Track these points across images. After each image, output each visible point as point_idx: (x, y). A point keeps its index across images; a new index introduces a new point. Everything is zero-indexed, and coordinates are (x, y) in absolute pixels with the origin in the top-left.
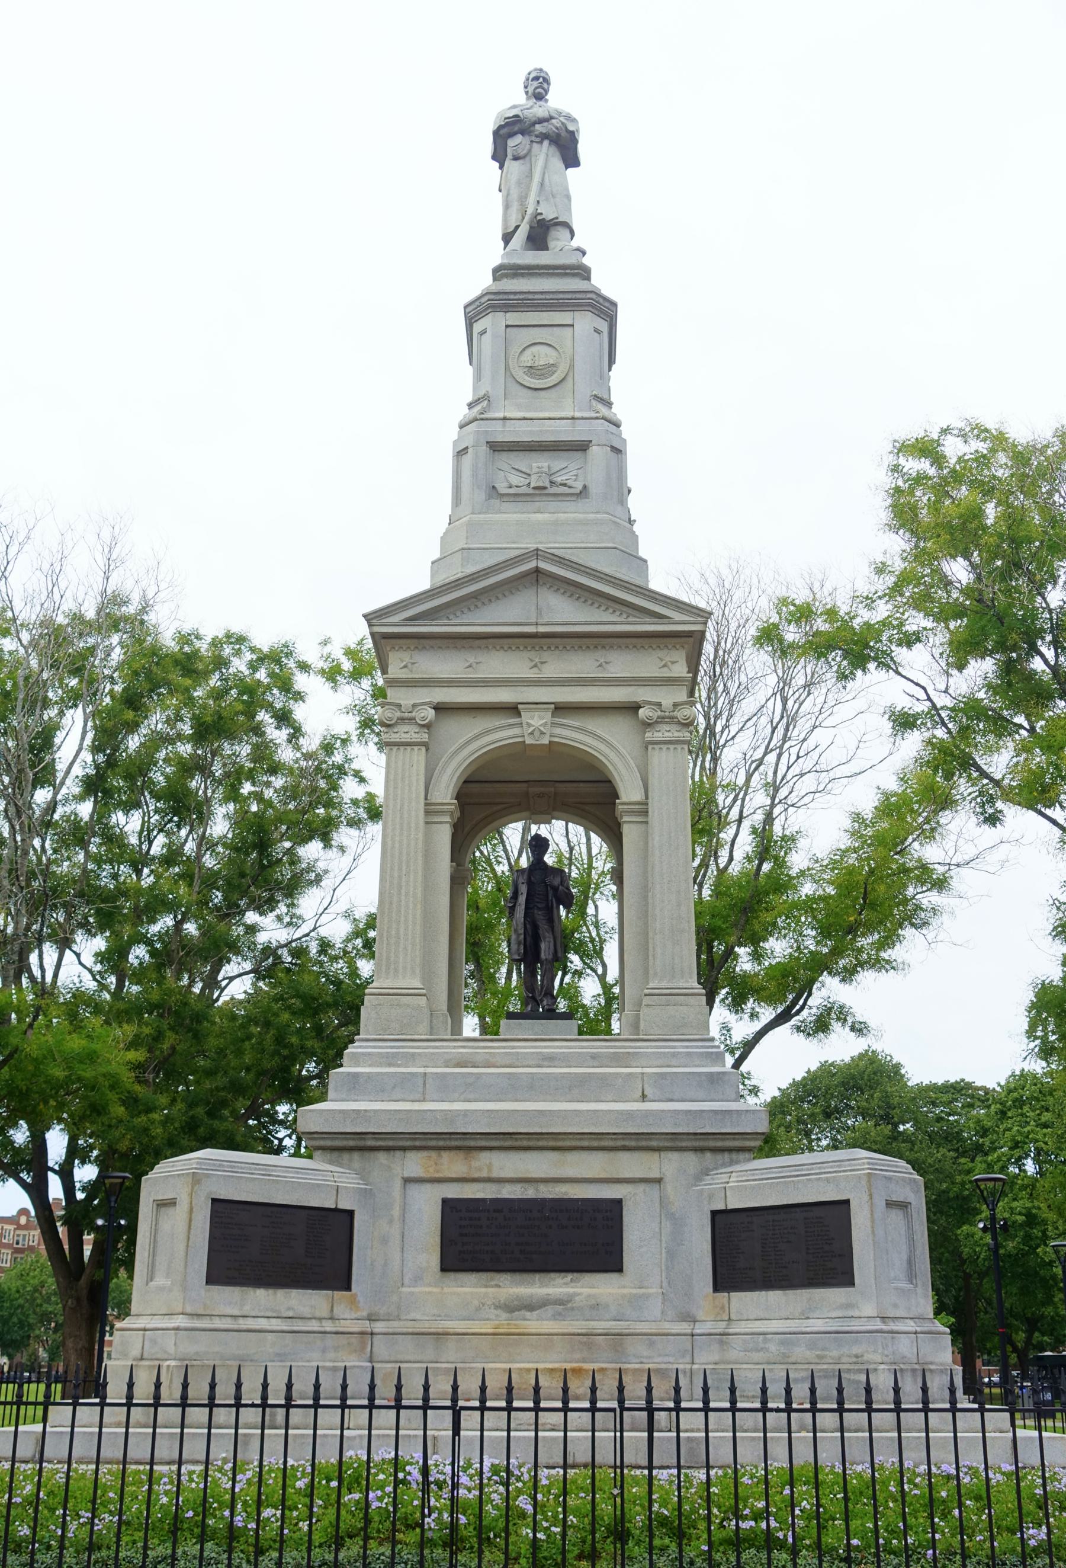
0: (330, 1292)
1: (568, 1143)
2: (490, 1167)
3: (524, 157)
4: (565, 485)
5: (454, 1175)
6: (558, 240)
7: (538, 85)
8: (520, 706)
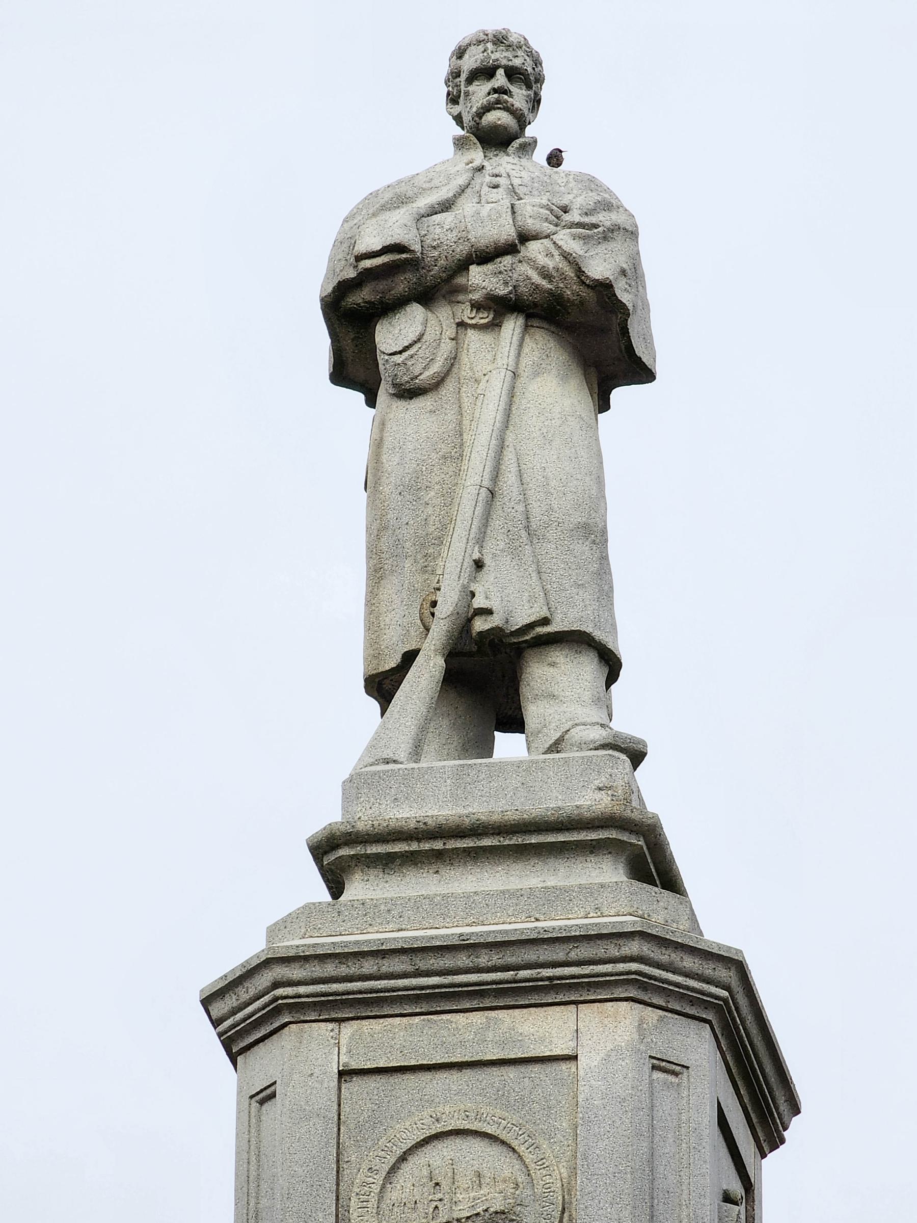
3: (436, 385)
6: (556, 688)
7: (496, 94)
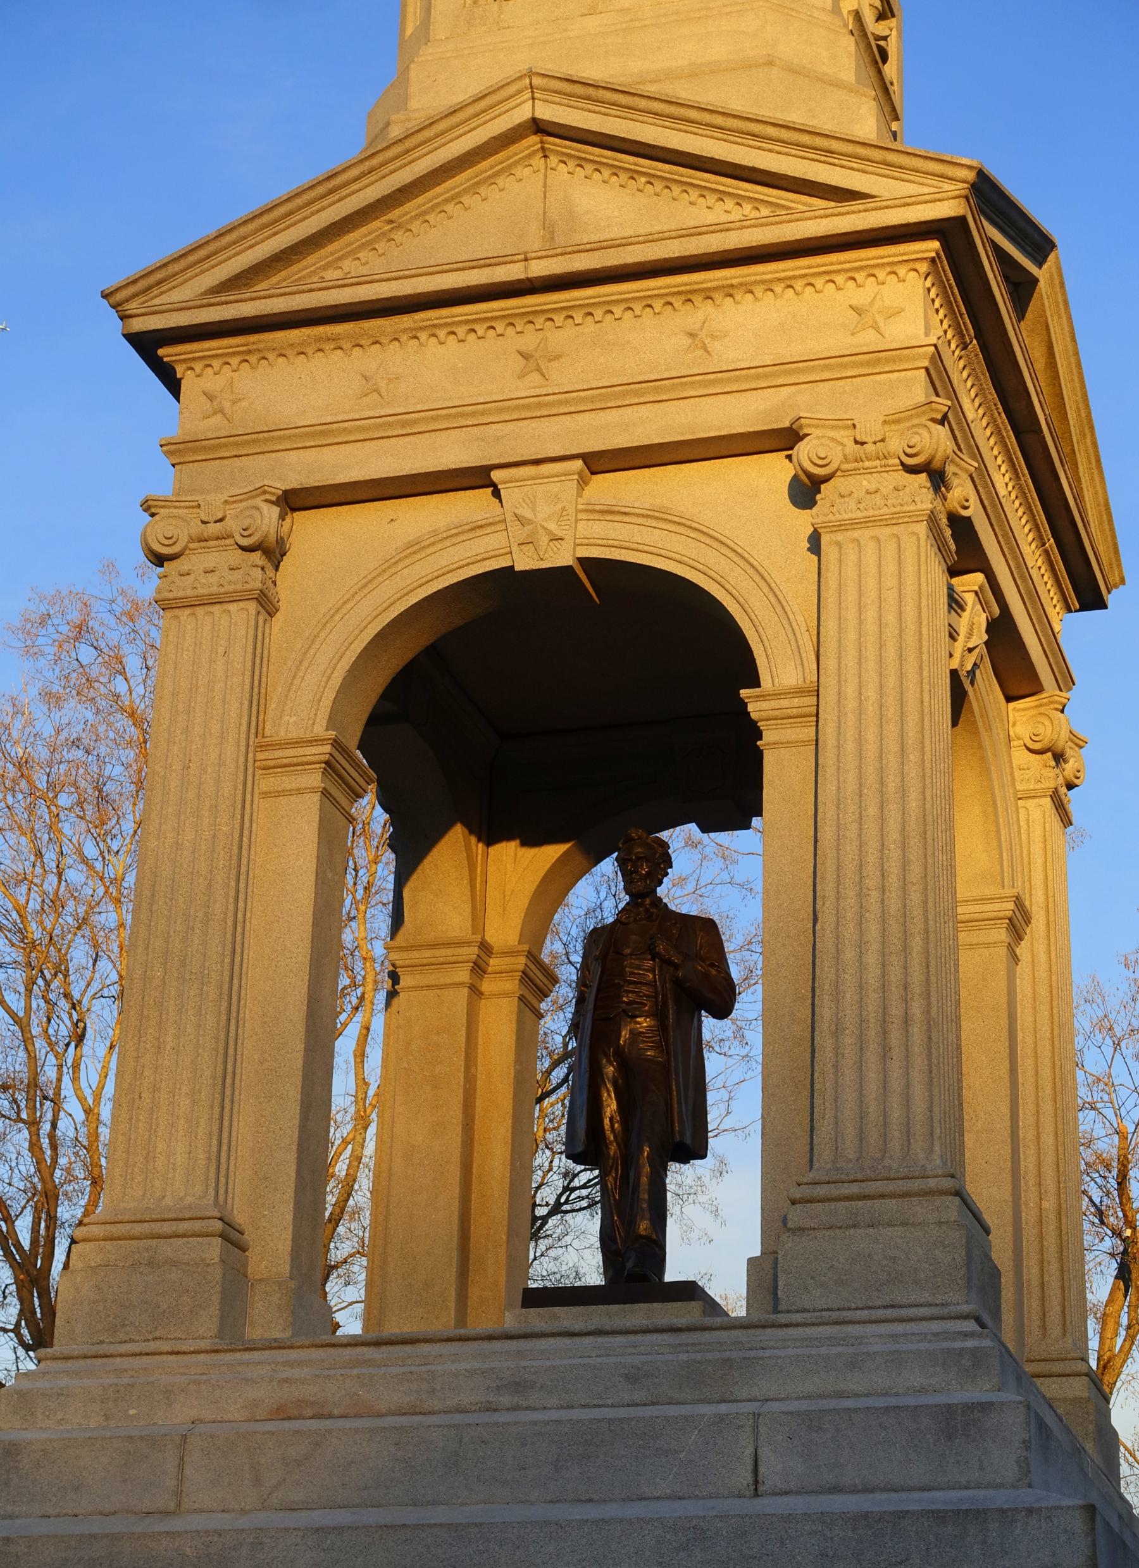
8: (496, 475)
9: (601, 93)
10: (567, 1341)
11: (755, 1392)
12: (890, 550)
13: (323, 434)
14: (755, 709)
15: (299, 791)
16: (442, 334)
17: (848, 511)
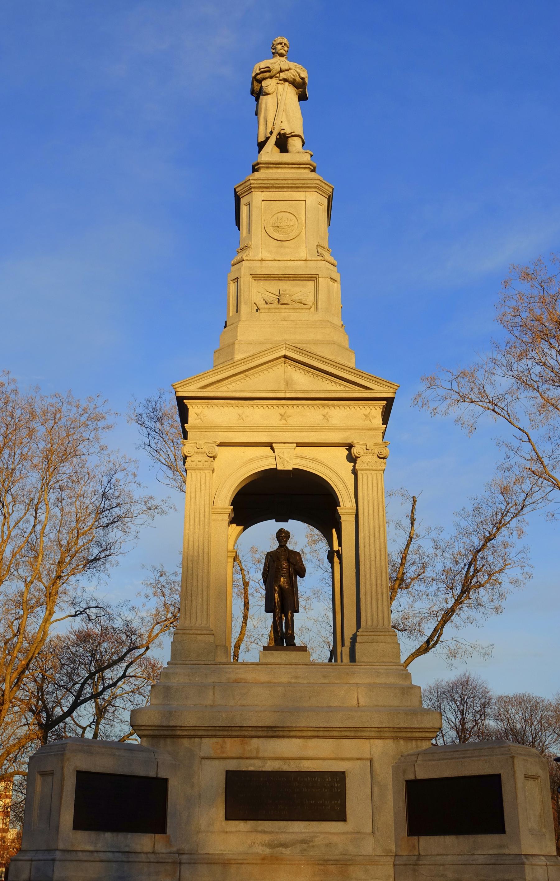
0: (153, 835)
1: (309, 734)
2: (258, 750)
4: (302, 303)
5: (234, 755)
8: (274, 445)
9: (304, 352)
10: (306, 666)
11: (354, 682)
12: (375, 477)
13: (229, 429)
14: (340, 512)
15: (222, 520)
16: (259, 406)
17: (365, 466)
